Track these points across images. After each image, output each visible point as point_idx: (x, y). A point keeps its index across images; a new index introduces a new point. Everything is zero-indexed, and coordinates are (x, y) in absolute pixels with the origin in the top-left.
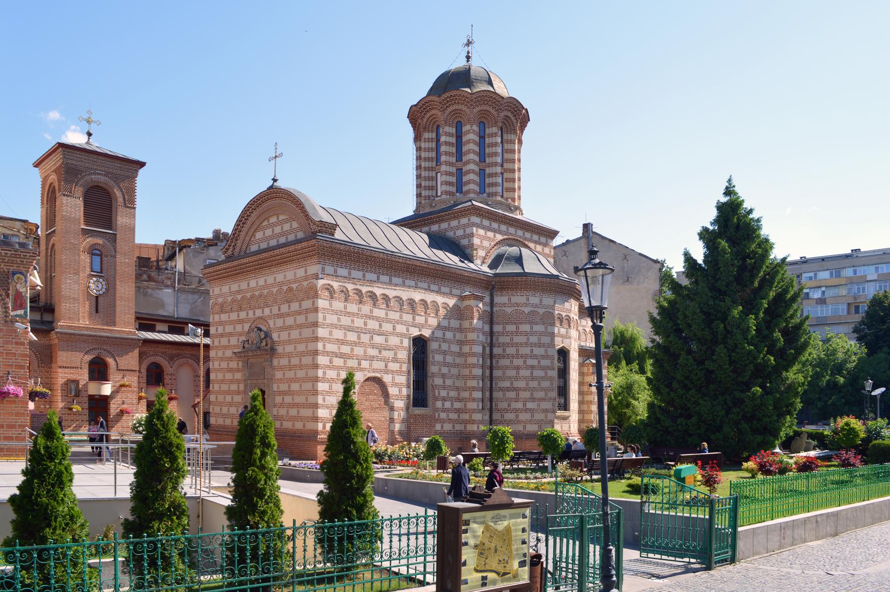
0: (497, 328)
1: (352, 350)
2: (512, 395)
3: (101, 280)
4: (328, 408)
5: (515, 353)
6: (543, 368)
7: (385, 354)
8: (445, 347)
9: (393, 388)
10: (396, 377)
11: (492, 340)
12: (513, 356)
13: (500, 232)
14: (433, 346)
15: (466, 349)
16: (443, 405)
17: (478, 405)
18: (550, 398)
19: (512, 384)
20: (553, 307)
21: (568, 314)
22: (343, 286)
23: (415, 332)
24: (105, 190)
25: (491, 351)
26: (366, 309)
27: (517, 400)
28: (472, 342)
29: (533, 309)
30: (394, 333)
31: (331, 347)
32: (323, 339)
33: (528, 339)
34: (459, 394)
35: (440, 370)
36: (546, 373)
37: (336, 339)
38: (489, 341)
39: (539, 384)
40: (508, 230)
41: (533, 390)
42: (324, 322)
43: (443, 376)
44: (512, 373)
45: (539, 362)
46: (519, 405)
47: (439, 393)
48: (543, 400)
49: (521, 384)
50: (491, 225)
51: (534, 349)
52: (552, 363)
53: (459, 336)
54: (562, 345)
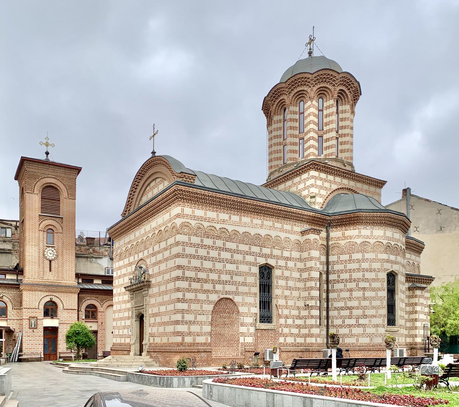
1: (208, 276)
2: (347, 313)
4: (186, 323)
5: (348, 278)
6: (373, 290)
7: (236, 278)
8: (287, 273)
10: (246, 298)
12: (346, 281)
13: (335, 183)
14: (276, 273)
15: (305, 275)
18: (381, 315)
23: (262, 261)
26: (219, 243)
28: (311, 269)
30: (244, 262)
33: (360, 265)
36: (377, 294)
37: (194, 267)
40: (342, 181)
41: (365, 308)
42: (184, 253)
45: (370, 285)
48: (375, 316)
50: (327, 177)
51: (365, 273)
52: (382, 285)
53: (300, 265)
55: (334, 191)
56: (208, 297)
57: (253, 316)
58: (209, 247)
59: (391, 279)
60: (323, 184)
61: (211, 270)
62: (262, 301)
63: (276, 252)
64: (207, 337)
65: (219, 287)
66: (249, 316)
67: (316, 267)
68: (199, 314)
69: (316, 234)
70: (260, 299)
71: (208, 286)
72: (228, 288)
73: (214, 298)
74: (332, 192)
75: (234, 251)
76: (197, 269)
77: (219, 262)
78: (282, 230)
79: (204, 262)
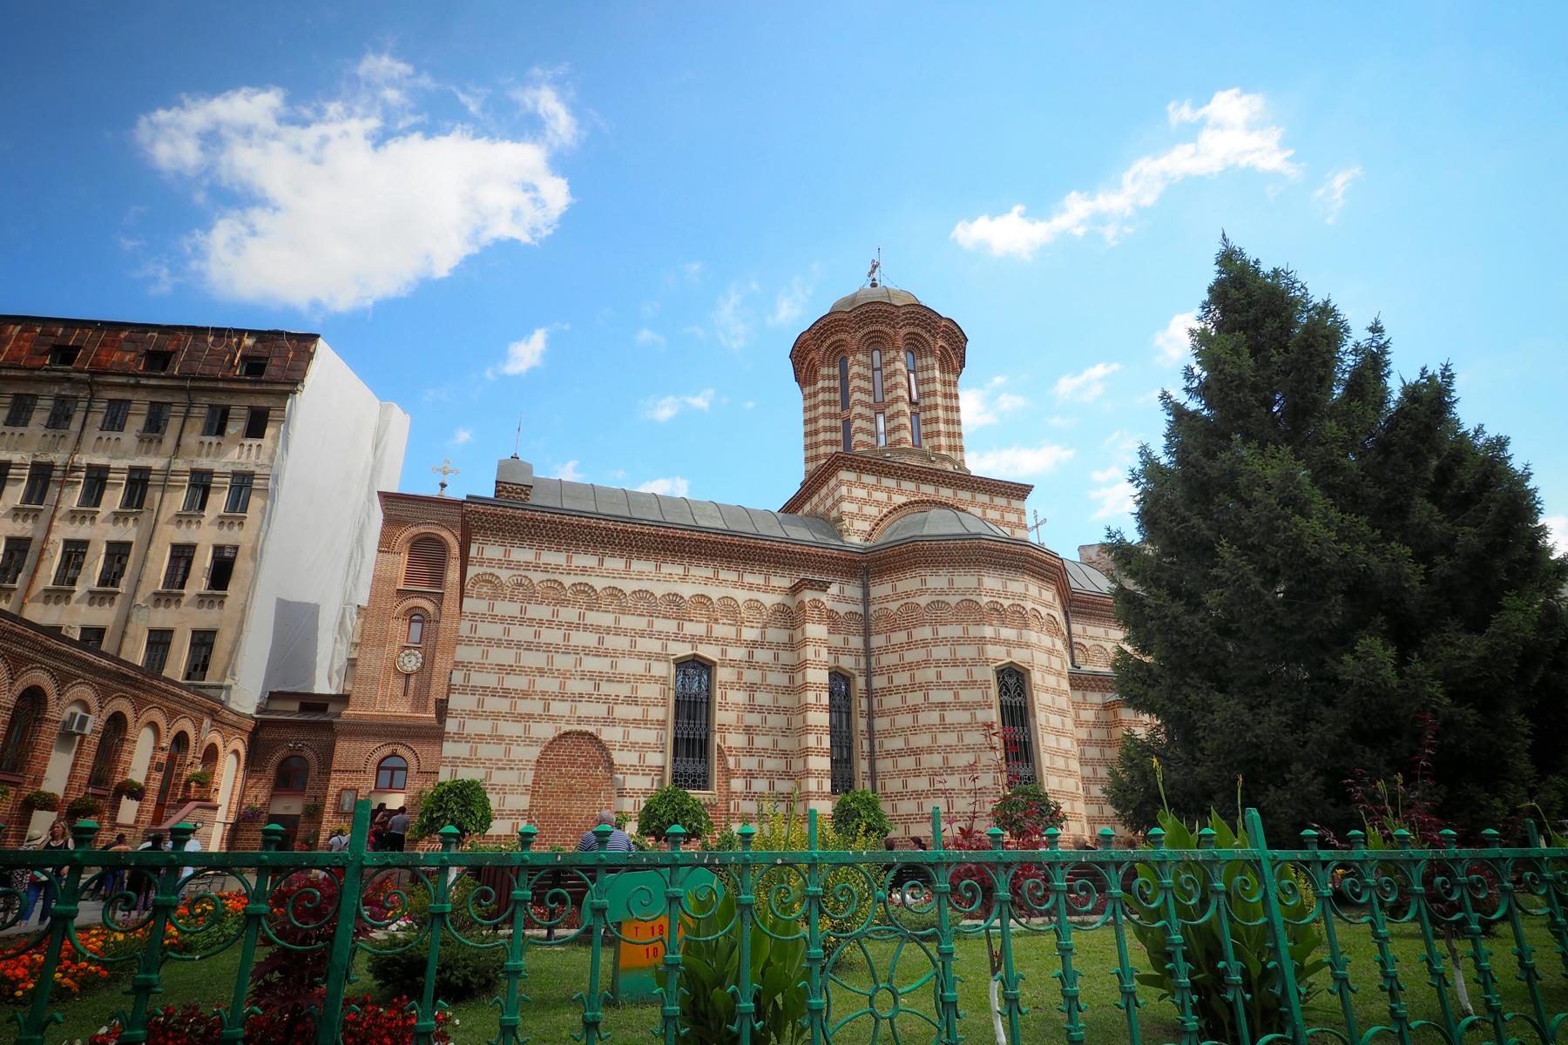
0: (877, 641)
2: (907, 763)
3: (417, 652)
5: (908, 682)
6: (965, 707)
7: (606, 688)
8: (751, 676)
9: (625, 753)
11: (868, 663)
12: (905, 688)
13: (901, 492)
16: (748, 785)
17: (820, 785)
19: (907, 741)
20: (978, 590)
23: (684, 650)
24: (439, 542)
25: (868, 683)
26: (569, 614)
27: (917, 773)
29: (935, 598)
30: (632, 653)
31: (478, 679)
33: (929, 653)
34: (789, 765)
38: (863, 665)
39: (960, 739)
42: (473, 635)
44: (905, 720)
45: (956, 695)
46: (922, 784)
47: (738, 763)
49: (923, 740)
51: (943, 670)
54: (1008, 660)
55: (899, 507)
56: (527, 729)
57: (653, 773)
58: (541, 623)
59: (1012, 681)
60: (869, 494)
61: (541, 671)
62: (682, 739)
63: (720, 630)
64: (516, 821)
65: (558, 708)
66: (641, 772)
67: (817, 659)
68: (499, 769)
69: (816, 590)
70: (676, 734)
71: (535, 707)
72: (584, 709)
73: (547, 731)
74: (895, 509)
75: (608, 630)
77: (563, 653)
79: (524, 654)
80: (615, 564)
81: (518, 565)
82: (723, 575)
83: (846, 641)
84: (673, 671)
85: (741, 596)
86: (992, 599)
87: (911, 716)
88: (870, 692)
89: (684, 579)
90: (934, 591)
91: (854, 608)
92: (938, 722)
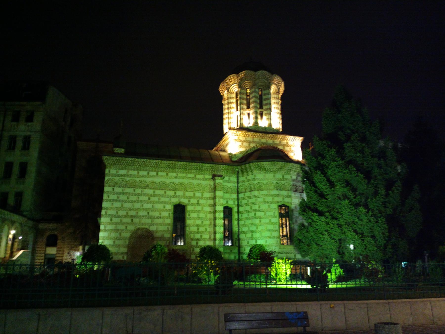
0: (241, 195)
1: (127, 213)
8: (198, 208)
18: (274, 237)
19: (249, 228)
21: (287, 182)
22: (122, 179)
23: (176, 201)
25: (238, 209)
29: (259, 181)
32: (106, 208)
35: (195, 222)
36: (270, 220)
38: (236, 204)
41: (262, 231)
43: (197, 225)
45: (265, 213)
47: (194, 236)
58: (129, 194)
61: (130, 209)
63: (188, 194)
75: (151, 195)
76: (117, 209)
78: (194, 178)
80: (153, 173)
81: (122, 175)
82: (190, 175)
83: (231, 196)
84: (173, 207)
85: (195, 182)
86: (278, 181)
87: (250, 220)
88: (238, 212)
89: (176, 177)
90: (259, 179)
91: (233, 185)
92: (258, 222)
